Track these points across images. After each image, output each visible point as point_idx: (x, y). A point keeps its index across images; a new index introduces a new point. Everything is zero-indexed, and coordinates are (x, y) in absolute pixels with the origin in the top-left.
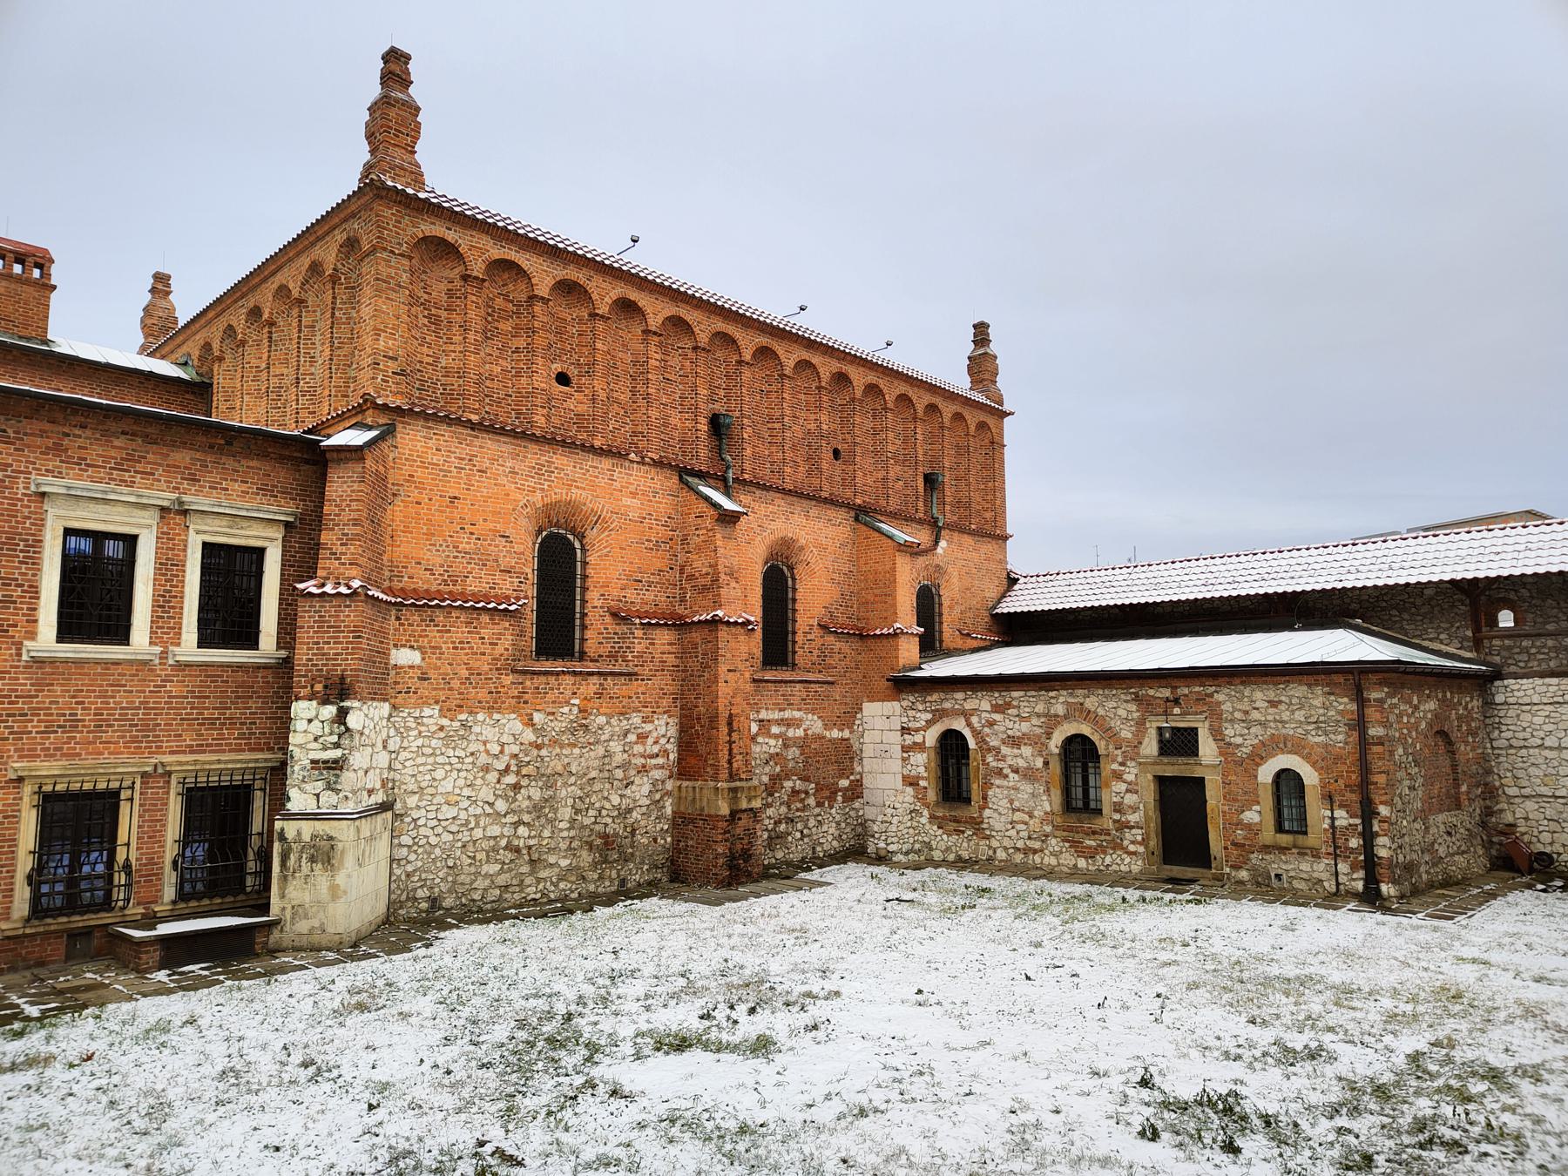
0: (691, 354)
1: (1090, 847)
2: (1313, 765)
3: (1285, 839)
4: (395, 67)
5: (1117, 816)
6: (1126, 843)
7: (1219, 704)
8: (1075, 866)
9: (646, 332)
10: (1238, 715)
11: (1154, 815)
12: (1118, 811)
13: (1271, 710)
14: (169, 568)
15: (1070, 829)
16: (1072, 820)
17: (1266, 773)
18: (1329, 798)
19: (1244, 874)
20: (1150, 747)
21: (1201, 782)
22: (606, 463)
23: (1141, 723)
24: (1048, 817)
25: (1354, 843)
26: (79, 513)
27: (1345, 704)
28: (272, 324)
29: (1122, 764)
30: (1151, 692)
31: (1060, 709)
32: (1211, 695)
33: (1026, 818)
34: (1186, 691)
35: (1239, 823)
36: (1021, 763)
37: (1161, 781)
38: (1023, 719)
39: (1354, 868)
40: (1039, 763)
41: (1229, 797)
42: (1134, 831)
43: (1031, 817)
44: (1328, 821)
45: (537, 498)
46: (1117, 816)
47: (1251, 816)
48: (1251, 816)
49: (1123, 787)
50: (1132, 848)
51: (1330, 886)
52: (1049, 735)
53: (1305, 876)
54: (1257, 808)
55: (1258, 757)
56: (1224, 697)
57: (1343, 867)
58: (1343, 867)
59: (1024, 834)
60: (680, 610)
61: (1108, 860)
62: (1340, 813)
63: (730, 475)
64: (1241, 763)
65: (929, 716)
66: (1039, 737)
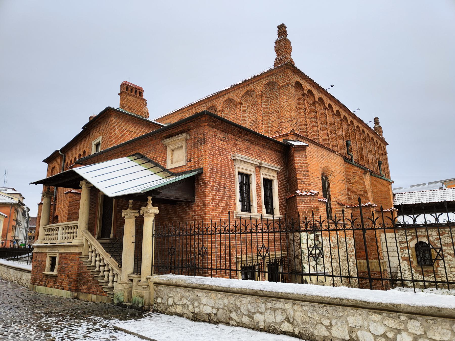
0: (340, 122)
4: (282, 30)
9: (333, 114)
14: (258, 185)
22: (332, 154)
26: (241, 167)
28: (222, 111)
45: (322, 166)
60: (350, 203)
63: (353, 159)
65: (411, 237)
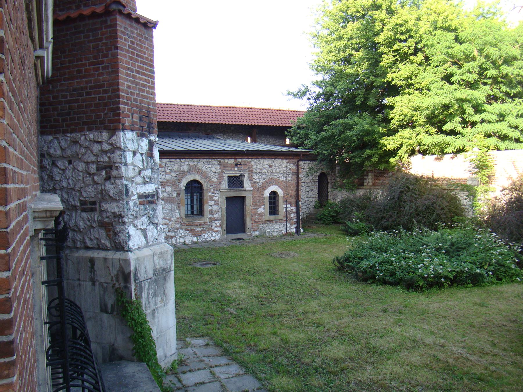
1: (198, 231)
2: (282, 189)
3: (272, 217)
5: (210, 216)
6: (213, 227)
7: (252, 166)
8: (192, 241)
10: (258, 170)
12: (210, 214)
13: (270, 169)
15: (189, 225)
16: (191, 220)
18: (286, 201)
20: (225, 185)
21: (244, 198)
23: (221, 175)
24: (179, 220)
25: (292, 216)
27: (292, 167)
29: (213, 193)
30: (226, 161)
31: (185, 168)
32: (249, 163)
33: (168, 221)
34: (240, 160)
35: (257, 213)
36: (165, 195)
37: (227, 198)
38: (167, 173)
39: (291, 225)
40: (175, 194)
41: (254, 204)
42: (216, 222)
43: (170, 221)
44: (285, 209)
46: (210, 216)
47: (261, 210)
48: (261, 210)
49: (213, 203)
50: (216, 229)
51: (284, 232)
52: (180, 181)
53: (276, 230)
54: (263, 207)
55: (264, 187)
56: (255, 163)
57: (288, 225)
58: (288, 225)
59: (167, 230)
61: (206, 236)
62: (288, 206)
66: (175, 182)
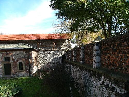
3: (20, 71)
11: (4, 69)
17: (18, 62)
18: (25, 65)
19: (15, 76)
20: (3, 60)
23: (2, 57)
34: (8, 52)
47: (16, 68)
55: (17, 61)
64: (15, 61)
